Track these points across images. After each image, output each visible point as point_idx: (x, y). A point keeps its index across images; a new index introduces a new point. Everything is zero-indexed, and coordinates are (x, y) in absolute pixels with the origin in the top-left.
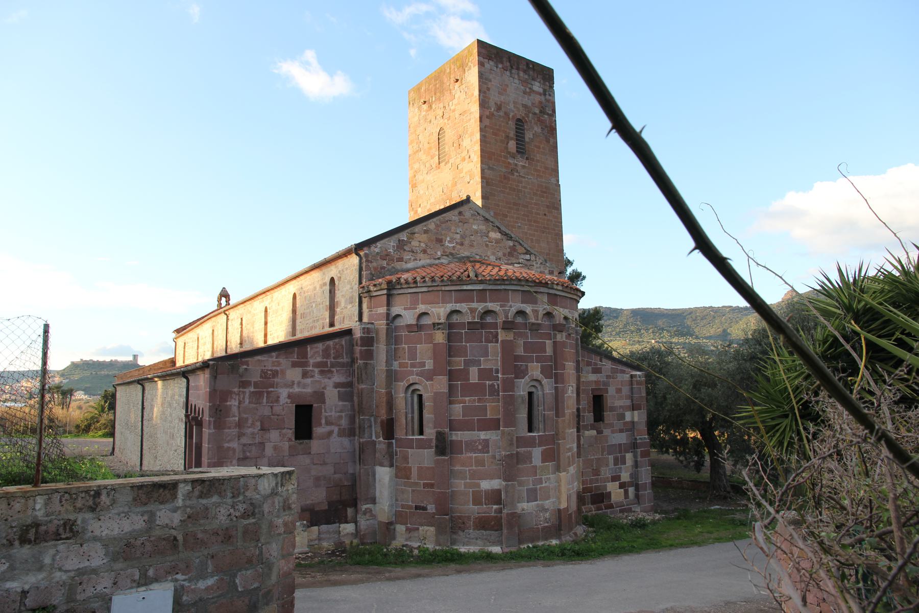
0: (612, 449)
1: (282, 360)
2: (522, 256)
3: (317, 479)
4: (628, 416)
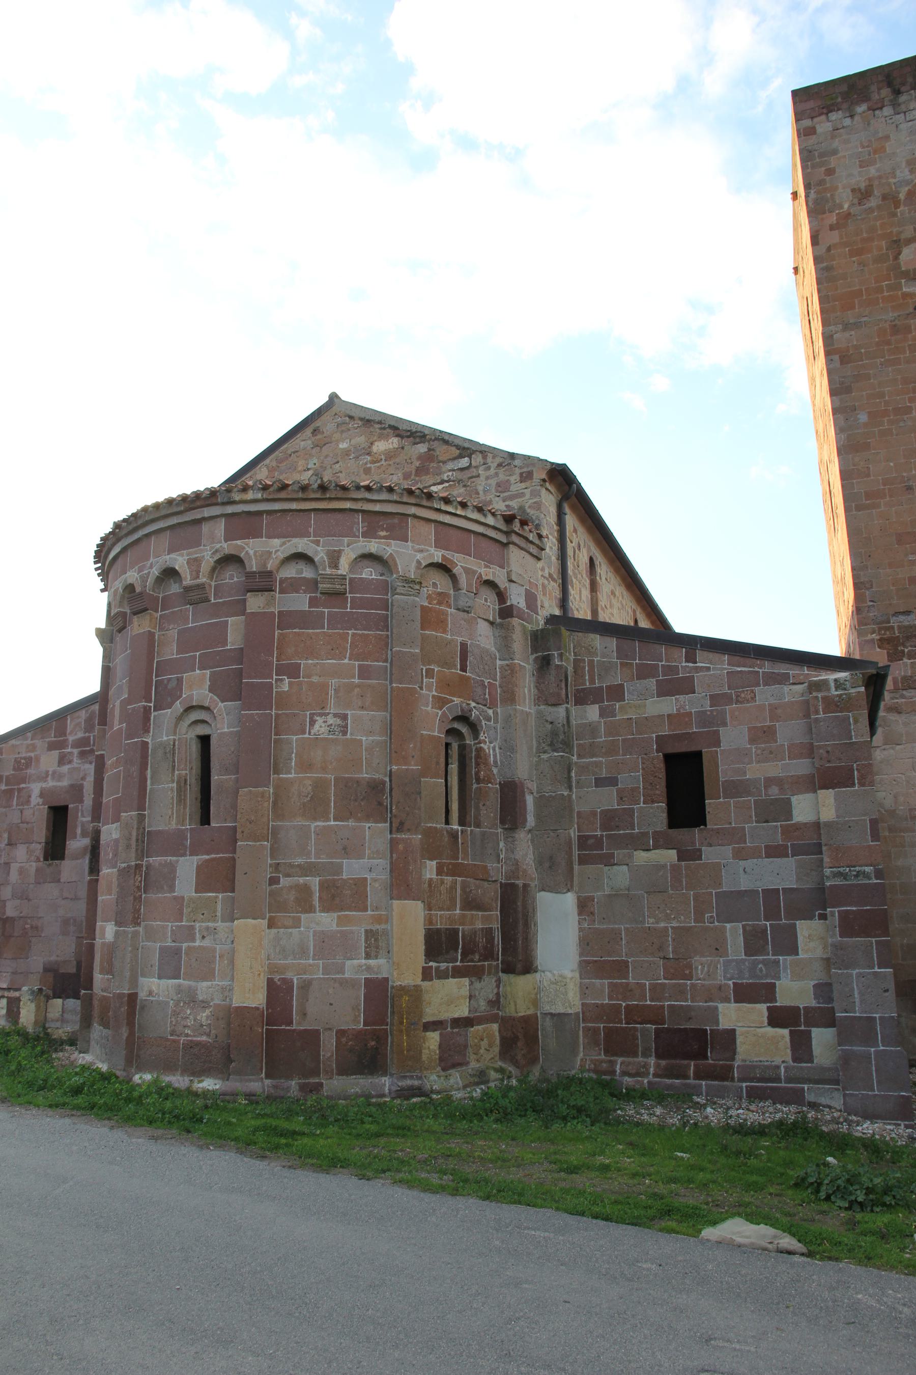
0: (734, 904)
1: (38, 742)
2: (450, 465)
3: (66, 922)
4: (805, 808)
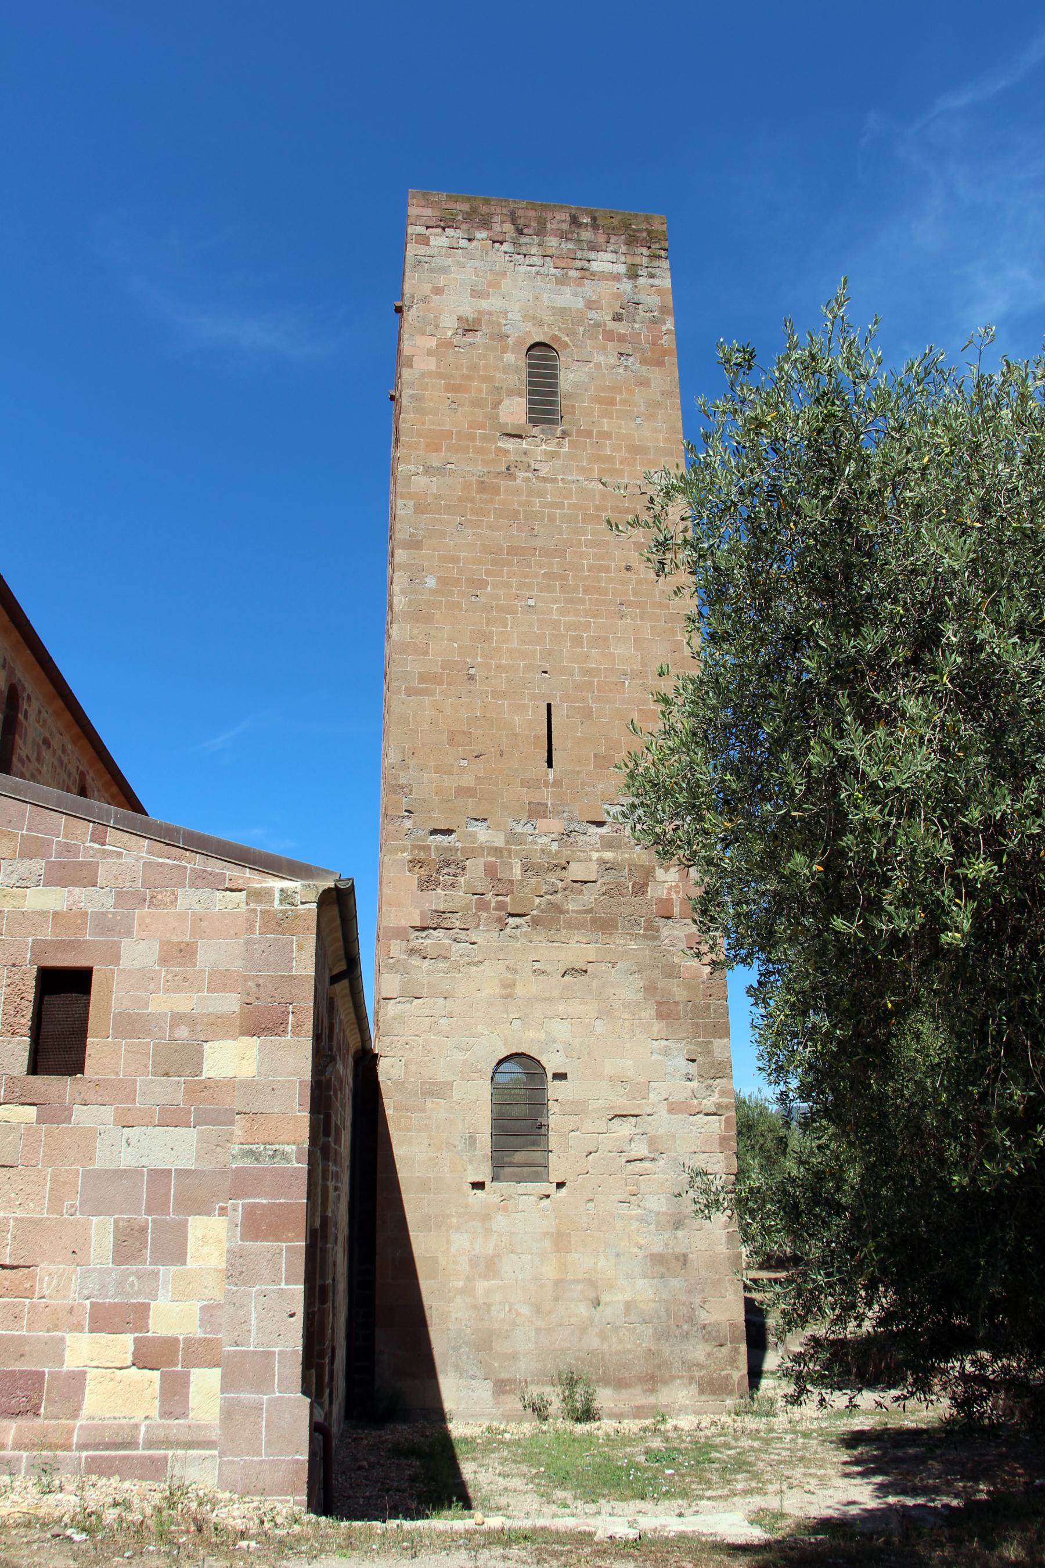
0: (105, 1188)
